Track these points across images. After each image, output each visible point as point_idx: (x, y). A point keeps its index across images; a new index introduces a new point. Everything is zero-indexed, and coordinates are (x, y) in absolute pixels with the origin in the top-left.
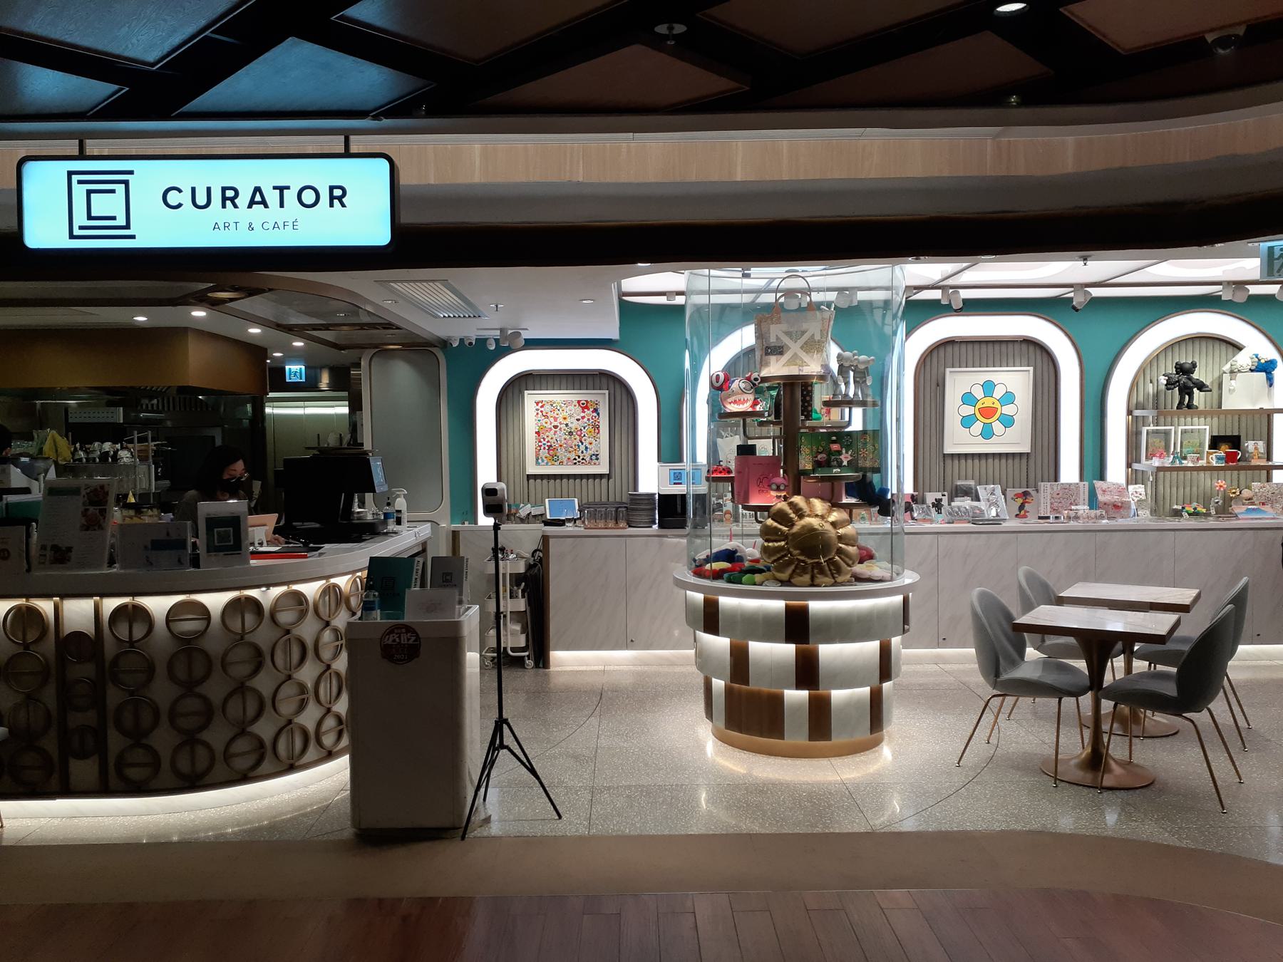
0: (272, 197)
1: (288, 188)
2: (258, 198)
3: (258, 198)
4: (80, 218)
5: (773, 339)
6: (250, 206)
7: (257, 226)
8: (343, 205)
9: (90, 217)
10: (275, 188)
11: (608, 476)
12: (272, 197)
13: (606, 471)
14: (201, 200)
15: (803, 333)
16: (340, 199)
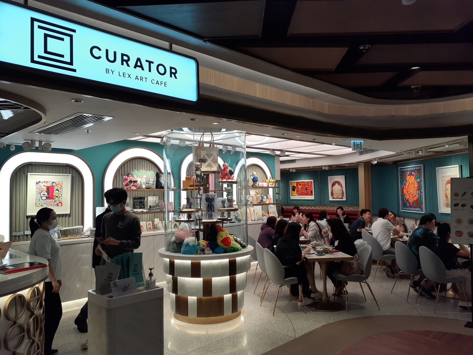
0: (146, 65)
1: (153, 63)
2: (139, 64)
3: (139, 64)
4: (39, 50)
5: (202, 157)
6: (135, 67)
7: (133, 77)
8: (176, 78)
9: (46, 52)
10: (147, 61)
11: (69, 215)
12: (146, 65)
13: (68, 212)
14: (111, 58)
15: (212, 155)
16: (175, 74)
